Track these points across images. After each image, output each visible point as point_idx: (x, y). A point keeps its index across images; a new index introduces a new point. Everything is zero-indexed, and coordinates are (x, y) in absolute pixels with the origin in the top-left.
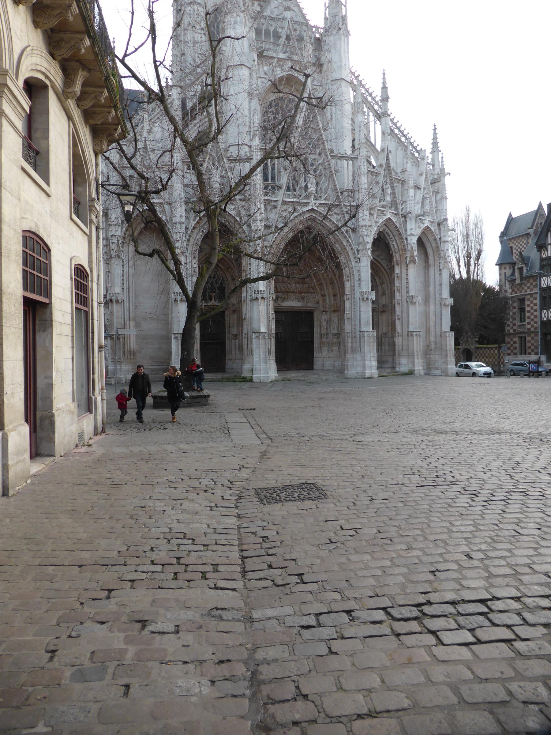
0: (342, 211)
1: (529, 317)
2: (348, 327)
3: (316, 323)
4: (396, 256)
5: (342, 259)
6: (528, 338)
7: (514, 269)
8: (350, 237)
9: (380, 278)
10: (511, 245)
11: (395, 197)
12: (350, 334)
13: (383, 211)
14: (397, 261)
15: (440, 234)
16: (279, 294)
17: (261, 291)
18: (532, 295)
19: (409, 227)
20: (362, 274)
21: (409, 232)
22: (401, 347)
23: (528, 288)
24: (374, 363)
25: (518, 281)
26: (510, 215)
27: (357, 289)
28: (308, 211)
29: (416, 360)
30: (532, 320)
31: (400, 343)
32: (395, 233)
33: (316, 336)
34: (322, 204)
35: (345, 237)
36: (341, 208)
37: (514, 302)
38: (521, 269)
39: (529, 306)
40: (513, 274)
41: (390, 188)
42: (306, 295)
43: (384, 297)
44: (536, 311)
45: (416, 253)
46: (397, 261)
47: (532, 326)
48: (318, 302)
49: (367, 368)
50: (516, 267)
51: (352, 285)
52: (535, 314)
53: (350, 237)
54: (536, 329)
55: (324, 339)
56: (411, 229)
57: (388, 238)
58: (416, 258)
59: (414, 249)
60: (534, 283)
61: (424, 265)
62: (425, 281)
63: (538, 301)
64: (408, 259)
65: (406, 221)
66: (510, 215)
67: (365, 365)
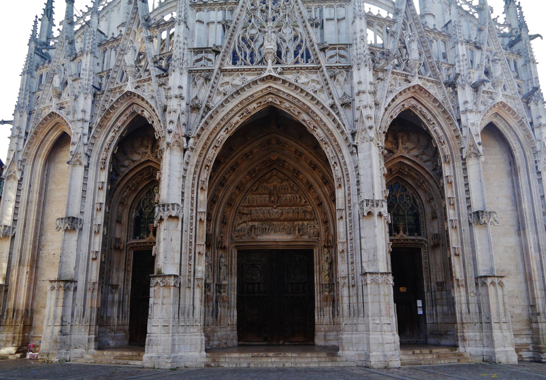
0: (324, 76)
2: (342, 268)
3: (316, 268)
4: (444, 150)
5: (329, 152)
8: (338, 114)
9: (425, 192)
11: (430, 57)
12: (346, 281)
13: (406, 76)
14: (445, 156)
15: (530, 115)
16: (256, 224)
17: (168, 205)
19: (461, 101)
20: (361, 172)
21: (462, 109)
22: (464, 307)
24: (392, 337)
27: (355, 199)
28: (263, 80)
29: (497, 334)
31: (463, 299)
32: (435, 111)
33: (317, 288)
34: (289, 68)
35: (329, 114)
36: (322, 71)
41: (416, 42)
42: (300, 223)
45: (478, 140)
46: (445, 156)
48: (318, 235)
49: (373, 347)
51: (347, 192)
53: (338, 114)
55: (327, 293)
56: (466, 102)
57: (425, 121)
58: (480, 148)
59: (473, 133)
61: (509, 169)
62: (514, 194)
65: (456, 93)
67: (368, 339)
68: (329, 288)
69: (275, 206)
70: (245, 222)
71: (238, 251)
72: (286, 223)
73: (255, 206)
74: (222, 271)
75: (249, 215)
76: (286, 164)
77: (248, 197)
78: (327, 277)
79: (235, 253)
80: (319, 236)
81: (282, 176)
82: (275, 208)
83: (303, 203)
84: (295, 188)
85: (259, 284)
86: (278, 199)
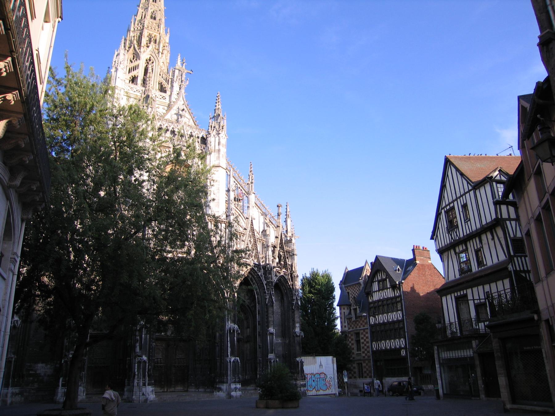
1: (363, 348)
6: (364, 365)
7: (351, 310)
10: (348, 291)
14: (258, 301)
18: (364, 330)
23: (361, 324)
25: (354, 319)
26: (346, 268)
30: (366, 350)
37: (352, 335)
38: (355, 310)
39: (362, 338)
40: (350, 313)
43: (248, 330)
44: (368, 342)
47: (366, 355)
50: (352, 308)
52: (367, 345)
54: (369, 357)
60: (365, 321)
63: (369, 335)
64: (267, 300)
66: (346, 268)
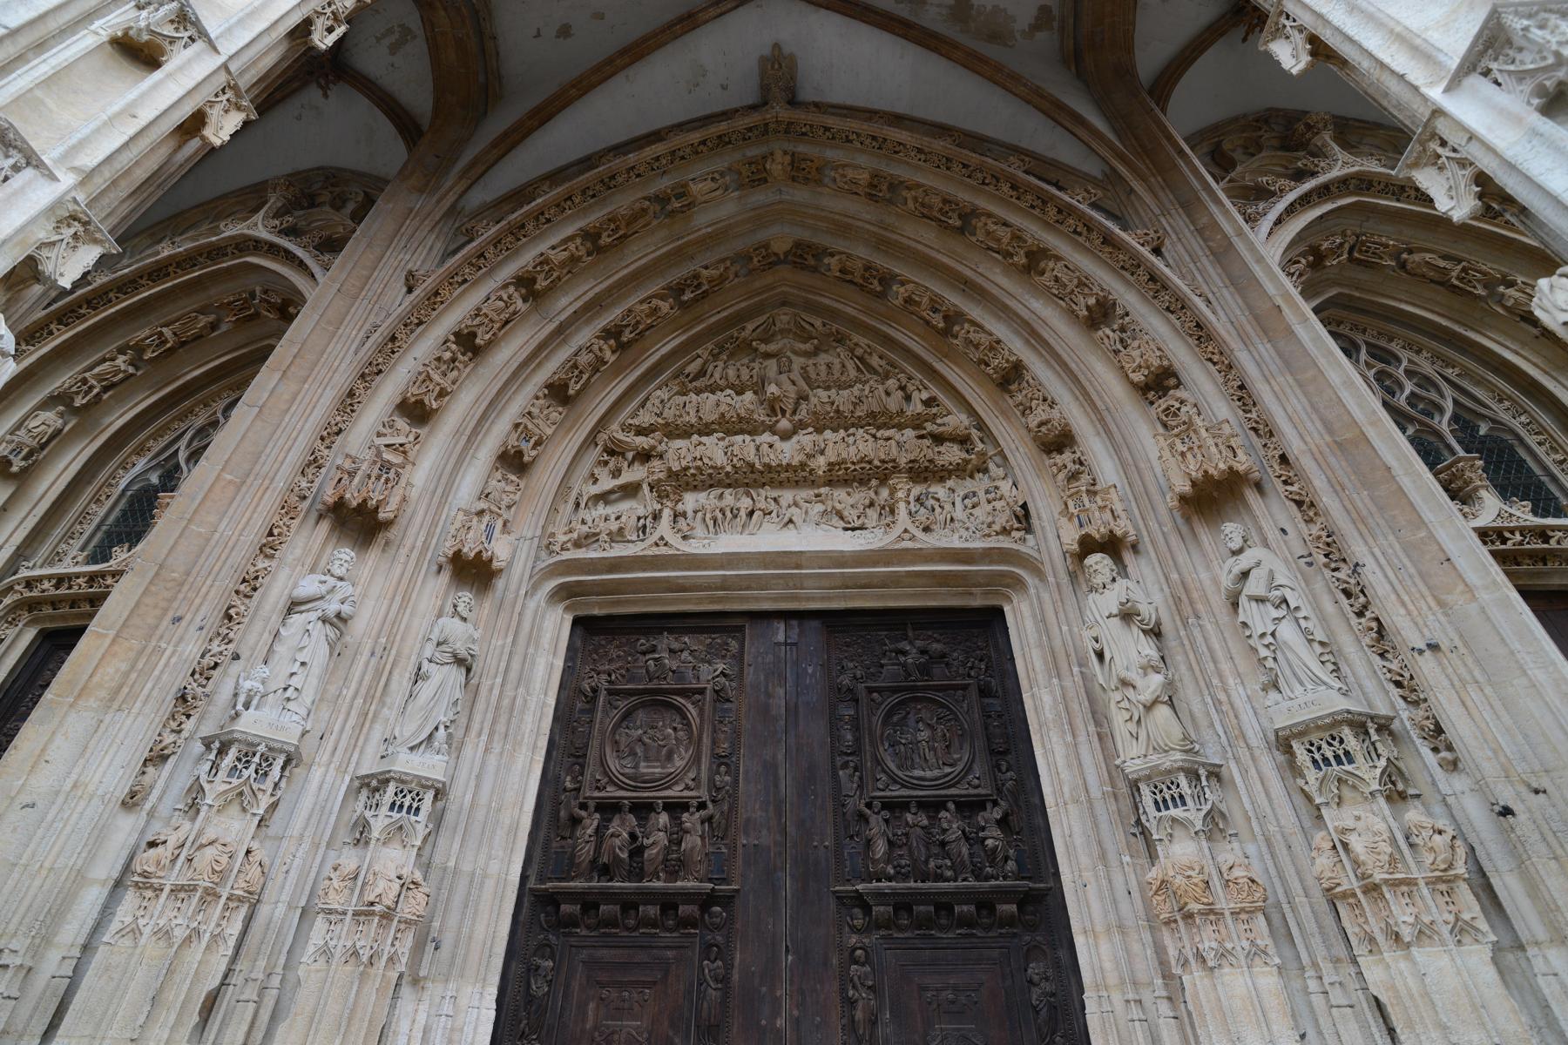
48: (1024, 517)
68: (1200, 798)
69: (784, 424)
70: (630, 491)
71: (577, 622)
72: (840, 494)
73: (685, 433)
74: (426, 690)
75: (656, 463)
76: (833, 262)
77: (659, 392)
78: (1163, 711)
79: (556, 626)
80: (1029, 530)
81: (818, 323)
82: (786, 436)
83: (920, 408)
84: (875, 361)
85: (676, 808)
86: (797, 404)
